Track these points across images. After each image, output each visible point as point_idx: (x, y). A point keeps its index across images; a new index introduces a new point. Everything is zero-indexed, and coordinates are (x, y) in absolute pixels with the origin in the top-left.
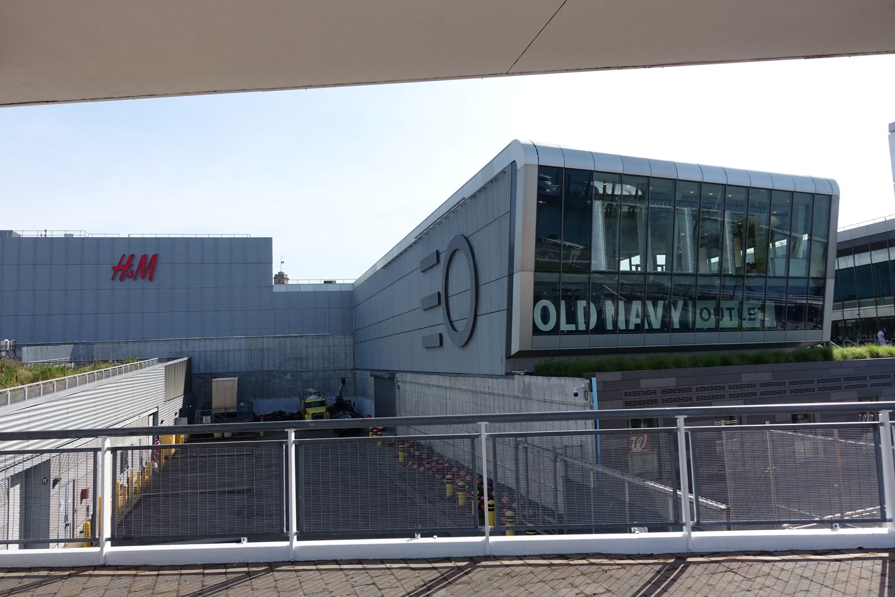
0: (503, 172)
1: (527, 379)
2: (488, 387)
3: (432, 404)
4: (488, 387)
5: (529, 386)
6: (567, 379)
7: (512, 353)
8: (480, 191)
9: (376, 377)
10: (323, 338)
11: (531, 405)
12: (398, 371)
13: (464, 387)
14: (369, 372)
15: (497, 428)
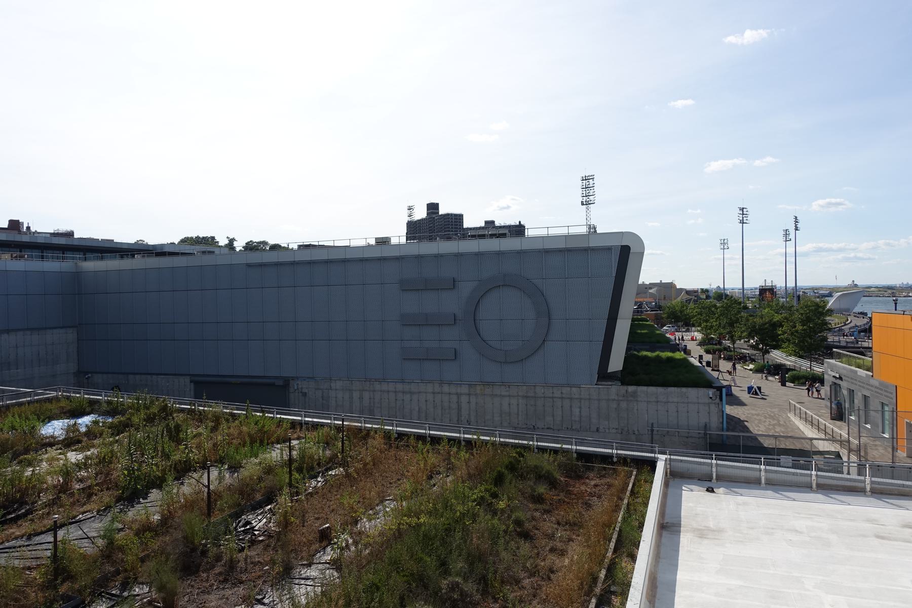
0: (609, 249)
1: (631, 389)
2: (562, 393)
3: (417, 409)
4: (562, 393)
5: (635, 392)
6: (690, 389)
7: (609, 371)
8: (560, 251)
9: (196, 383)
10: (39, 334)
11: (635, 404)
12: (297, 378)
13: (507, 393)
14: (189, 377)
15: (575, 421)
